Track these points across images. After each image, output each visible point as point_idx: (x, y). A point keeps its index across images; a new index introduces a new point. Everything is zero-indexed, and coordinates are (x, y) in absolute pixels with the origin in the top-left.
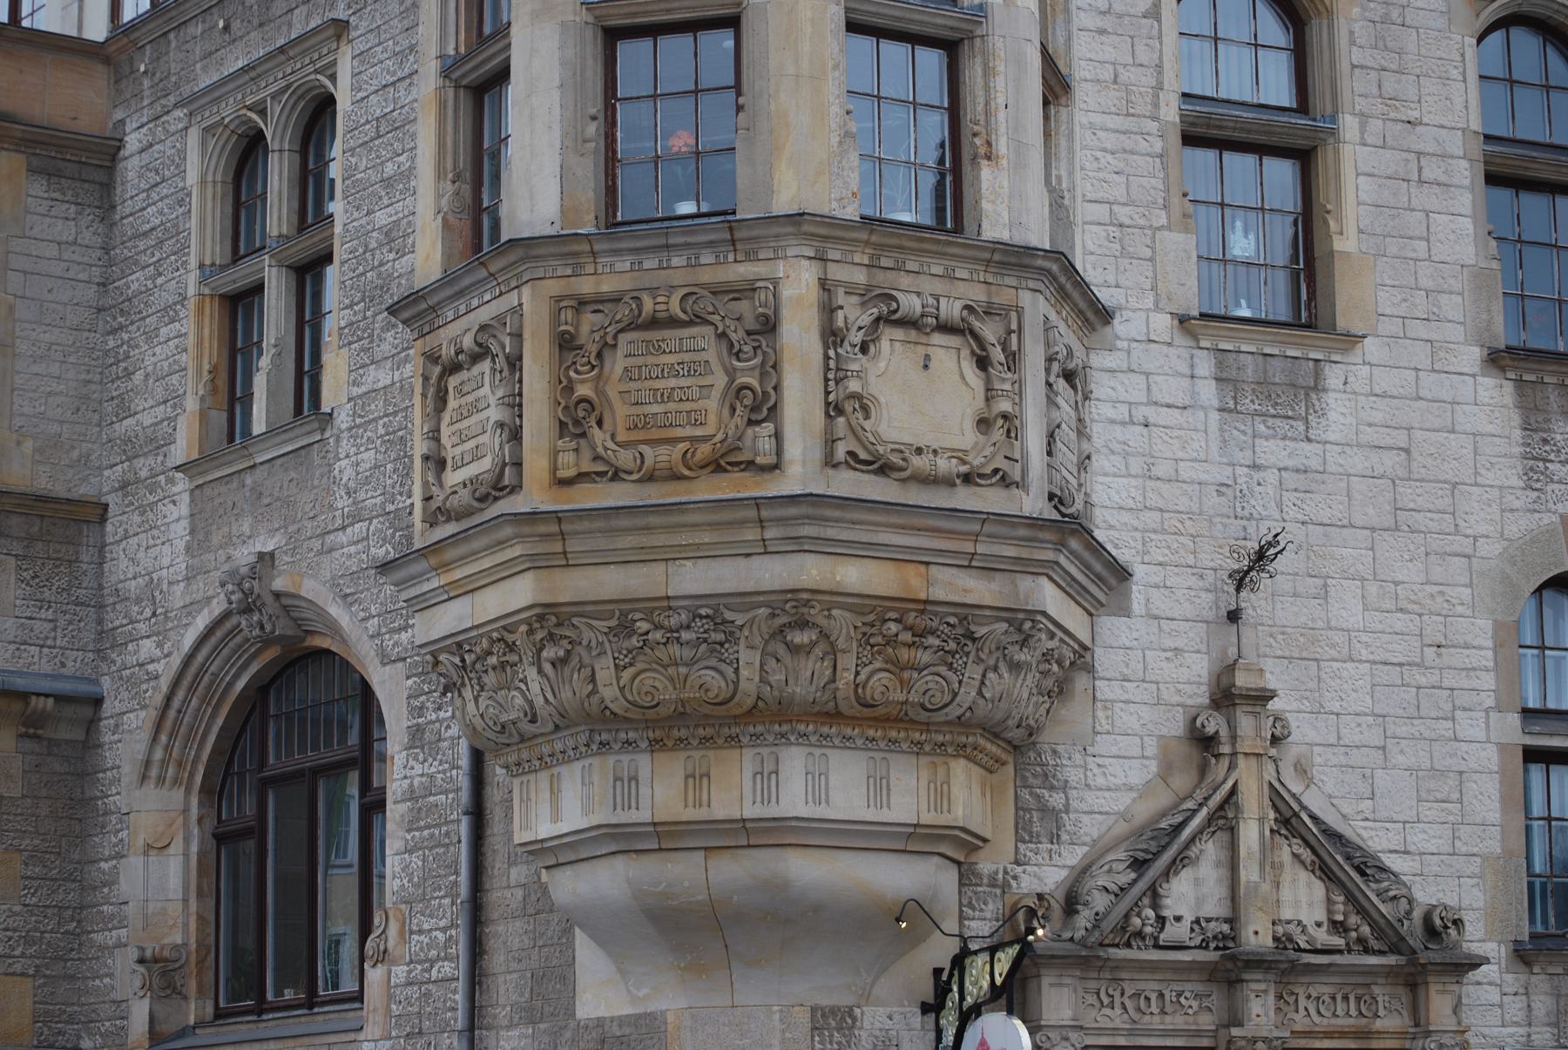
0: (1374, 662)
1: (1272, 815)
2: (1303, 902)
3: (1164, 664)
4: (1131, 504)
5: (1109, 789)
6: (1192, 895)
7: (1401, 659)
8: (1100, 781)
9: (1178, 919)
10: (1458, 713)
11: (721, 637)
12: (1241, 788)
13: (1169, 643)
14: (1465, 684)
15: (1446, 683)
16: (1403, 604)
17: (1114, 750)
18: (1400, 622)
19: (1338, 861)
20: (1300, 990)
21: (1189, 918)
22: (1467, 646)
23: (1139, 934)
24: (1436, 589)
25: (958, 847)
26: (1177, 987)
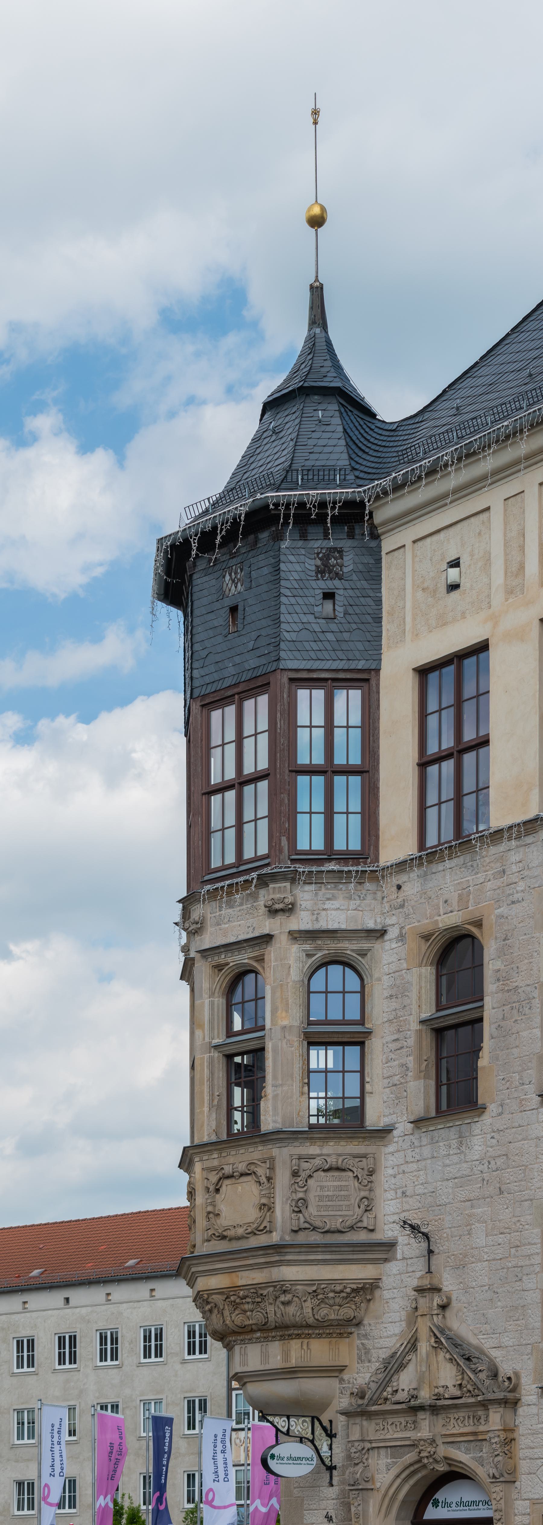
0: (489, 1261)
1: (433, 1340)
2: (447, 1376)
3: (408, 1279)
4: (397, 1210)
5: (388, 1337)
6: (406, 1380)
7: (501, 1256)
8: (385, 1334)
9: (403, 1390)
10: (525, 1278)
11: (259, 1300)
12: (419, 1330)
13: (410, 1269)
14: (528, 1262)
15: (520, 1264)
16: (503, 1230)
17: (390, 1320)
18: (501, 1239)
19: (466, 1356)
20: (451, 1416)
21: (406, 1389)
22: (530, 1244)
23: (386, 1399)
24: (517, 1219)
25: (337, 1371)
26: (407, 1419)
